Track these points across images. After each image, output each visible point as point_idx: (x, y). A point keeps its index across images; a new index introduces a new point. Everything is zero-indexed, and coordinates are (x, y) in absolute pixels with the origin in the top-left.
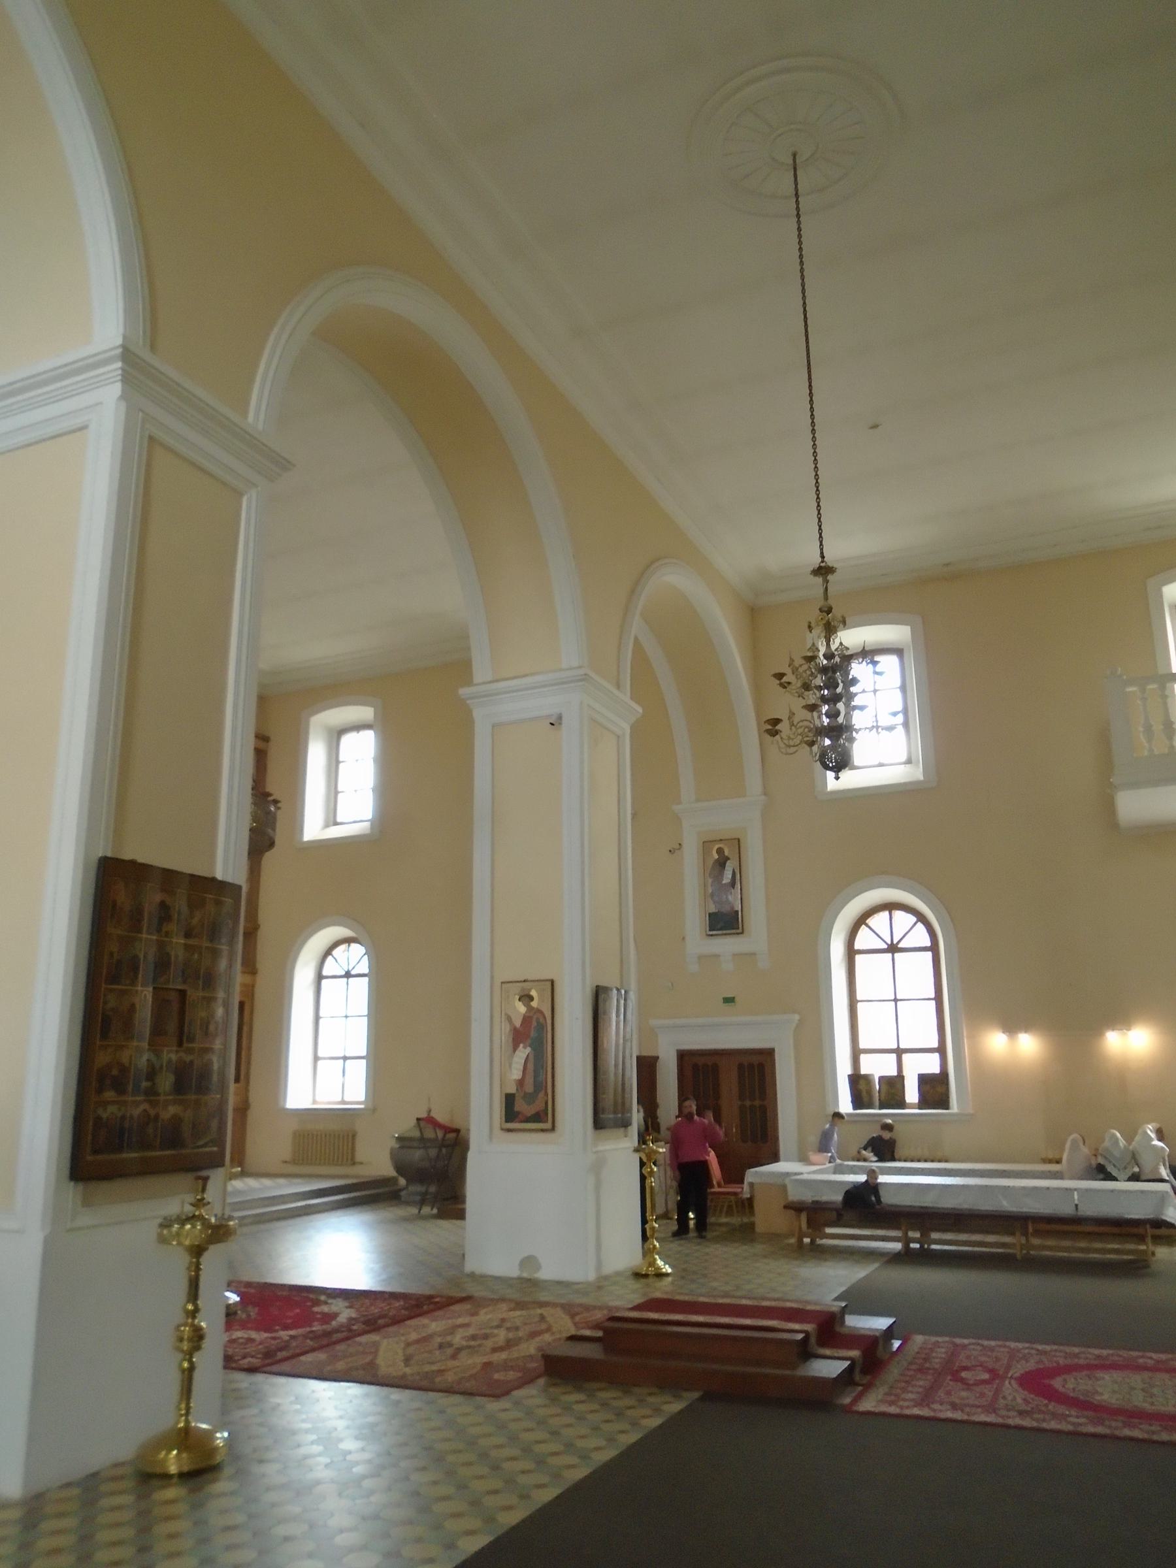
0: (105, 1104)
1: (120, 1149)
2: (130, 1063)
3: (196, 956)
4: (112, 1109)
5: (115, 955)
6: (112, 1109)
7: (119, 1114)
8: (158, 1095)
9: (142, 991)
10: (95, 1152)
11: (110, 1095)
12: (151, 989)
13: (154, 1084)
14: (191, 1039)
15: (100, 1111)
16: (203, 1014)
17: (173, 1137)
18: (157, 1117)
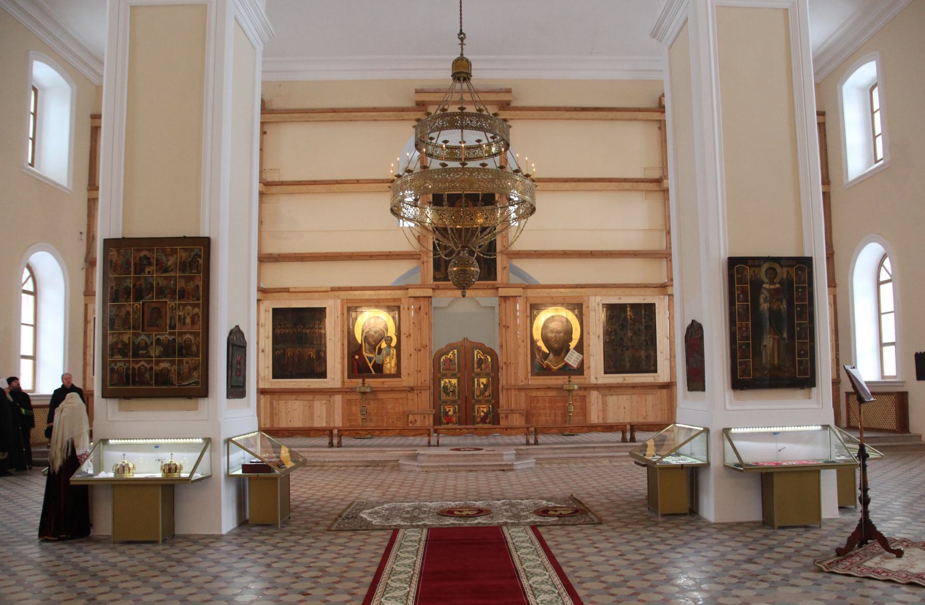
0: (116, 362)
1: (128, 384)
2: (129, 342)
3: (172, 282)
4: (119, 364)
5: (114, 288)
6: (119, 364)
7: (125, 367)
8: (152, 357)
9: (133, 305)
10: (112, 385)
11: (119, 357)
12: (141, 303)
13: (147, 352)
14: (173, 327)
15: (113, 365)
16: (181, 313)
17: (163, 379)
18: (151, 368)
